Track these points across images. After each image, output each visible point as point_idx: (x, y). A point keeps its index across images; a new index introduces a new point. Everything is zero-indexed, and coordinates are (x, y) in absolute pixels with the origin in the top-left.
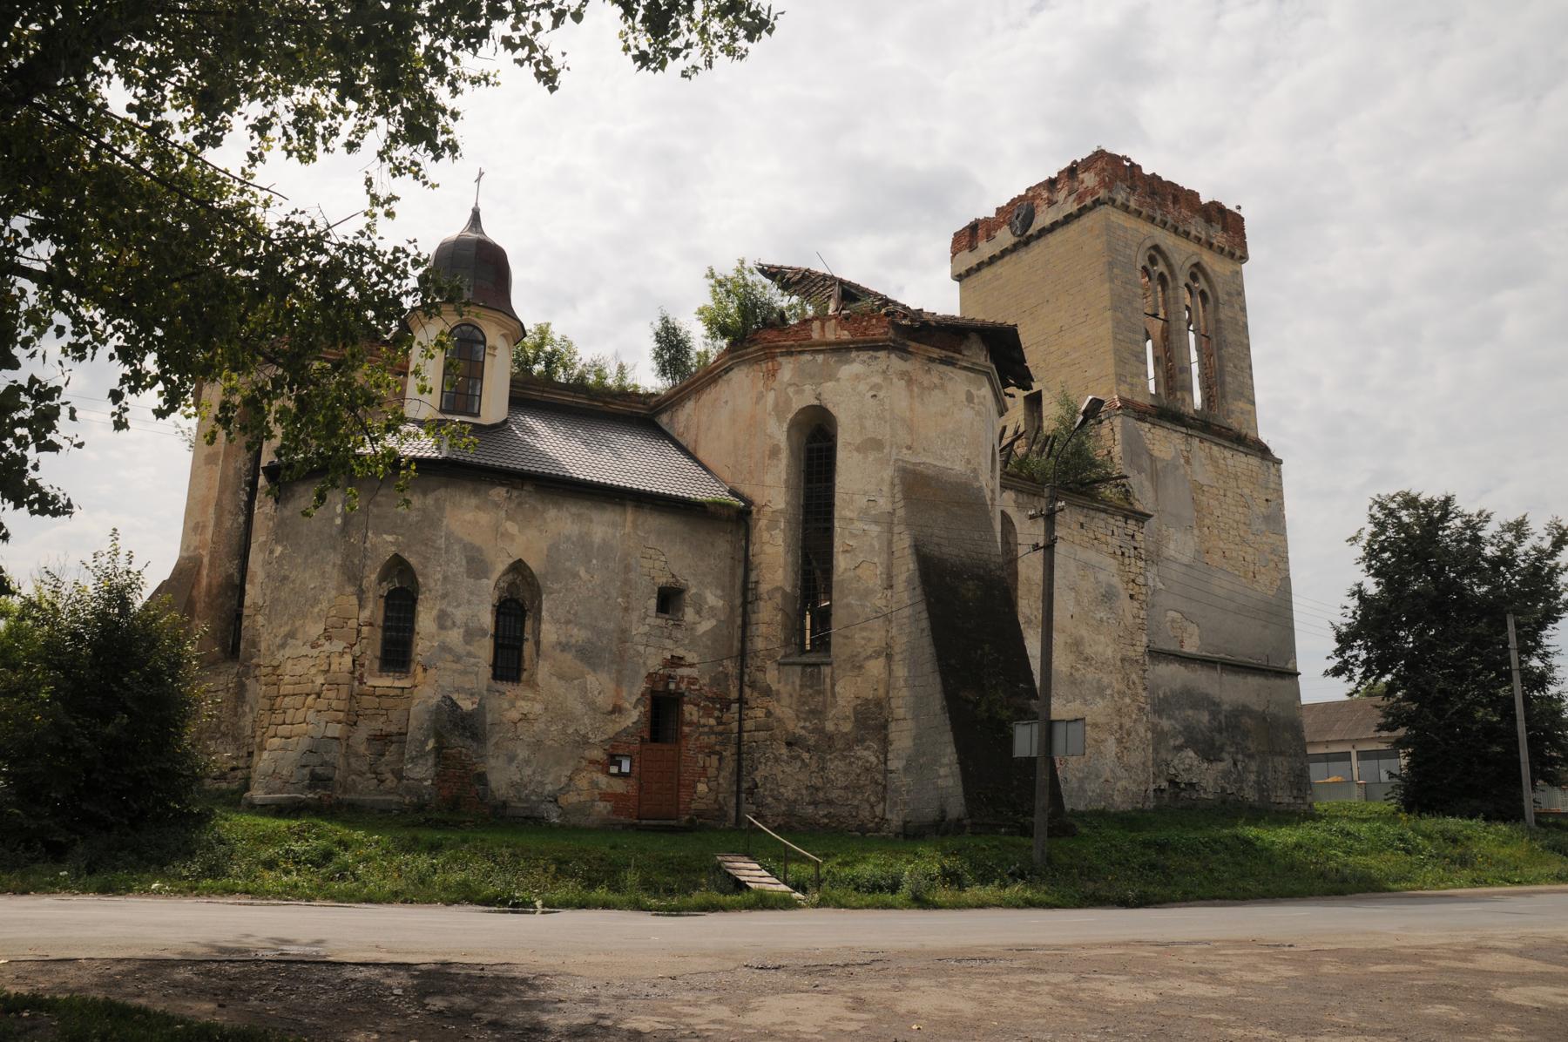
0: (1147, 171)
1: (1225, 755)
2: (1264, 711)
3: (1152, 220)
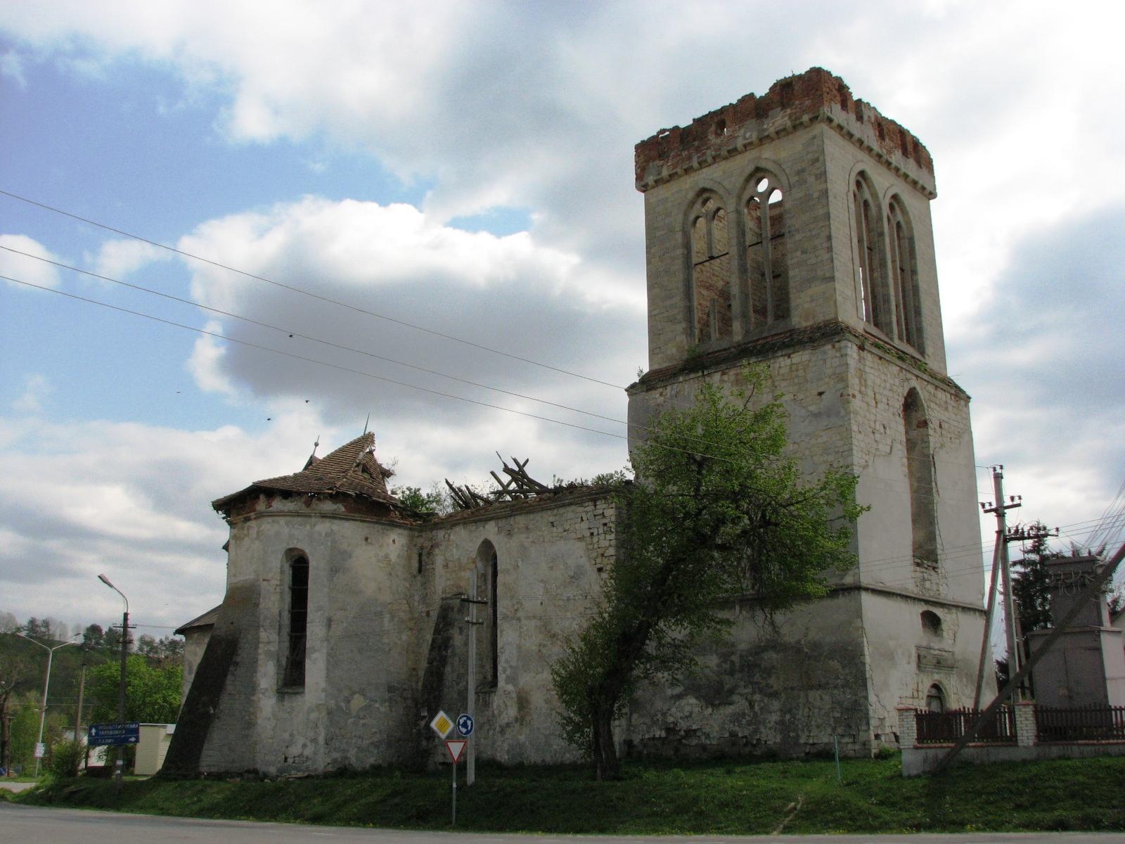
1: (735, 698)
2: (799, 642)
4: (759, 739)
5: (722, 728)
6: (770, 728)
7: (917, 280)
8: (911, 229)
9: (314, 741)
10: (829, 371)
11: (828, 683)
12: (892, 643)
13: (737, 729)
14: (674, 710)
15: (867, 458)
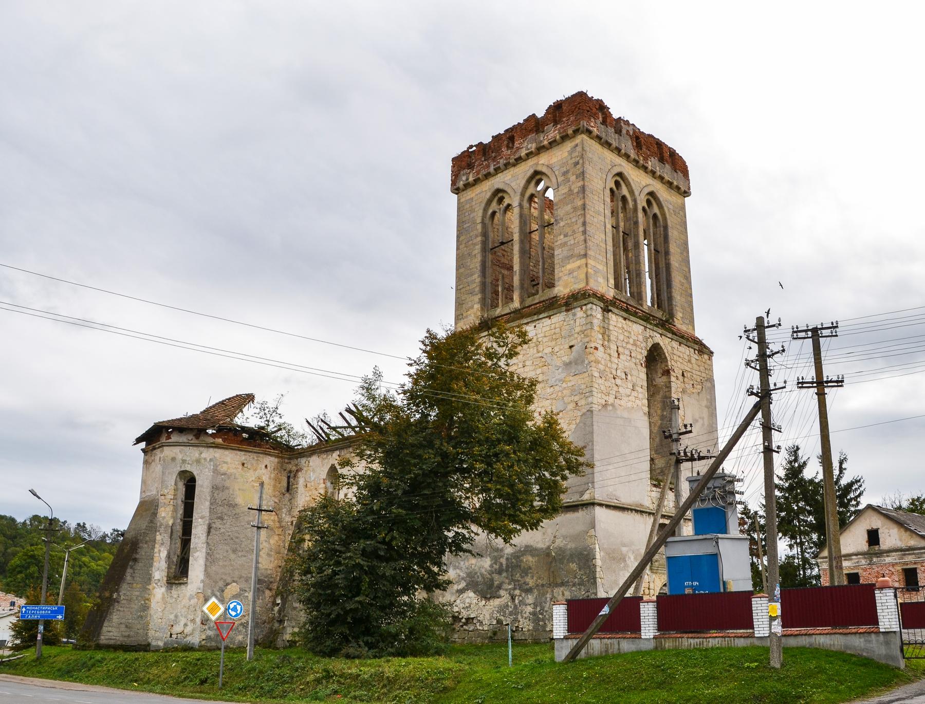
0: (487, 140)
1: (502, 593)
2: (549, 547)
3: (488, 176)
4: (518, 627)
5: (492, 617)
6: (526, 618)
7: (669, 259)
8: (665, 219)
9: (193, 621)
10: (578, 329)
11: (568, 582)
12: (624, 549)
13: (502, 618)
14: (458, 601)
15: (606, 398)
